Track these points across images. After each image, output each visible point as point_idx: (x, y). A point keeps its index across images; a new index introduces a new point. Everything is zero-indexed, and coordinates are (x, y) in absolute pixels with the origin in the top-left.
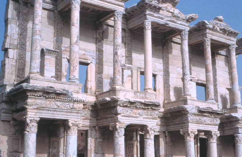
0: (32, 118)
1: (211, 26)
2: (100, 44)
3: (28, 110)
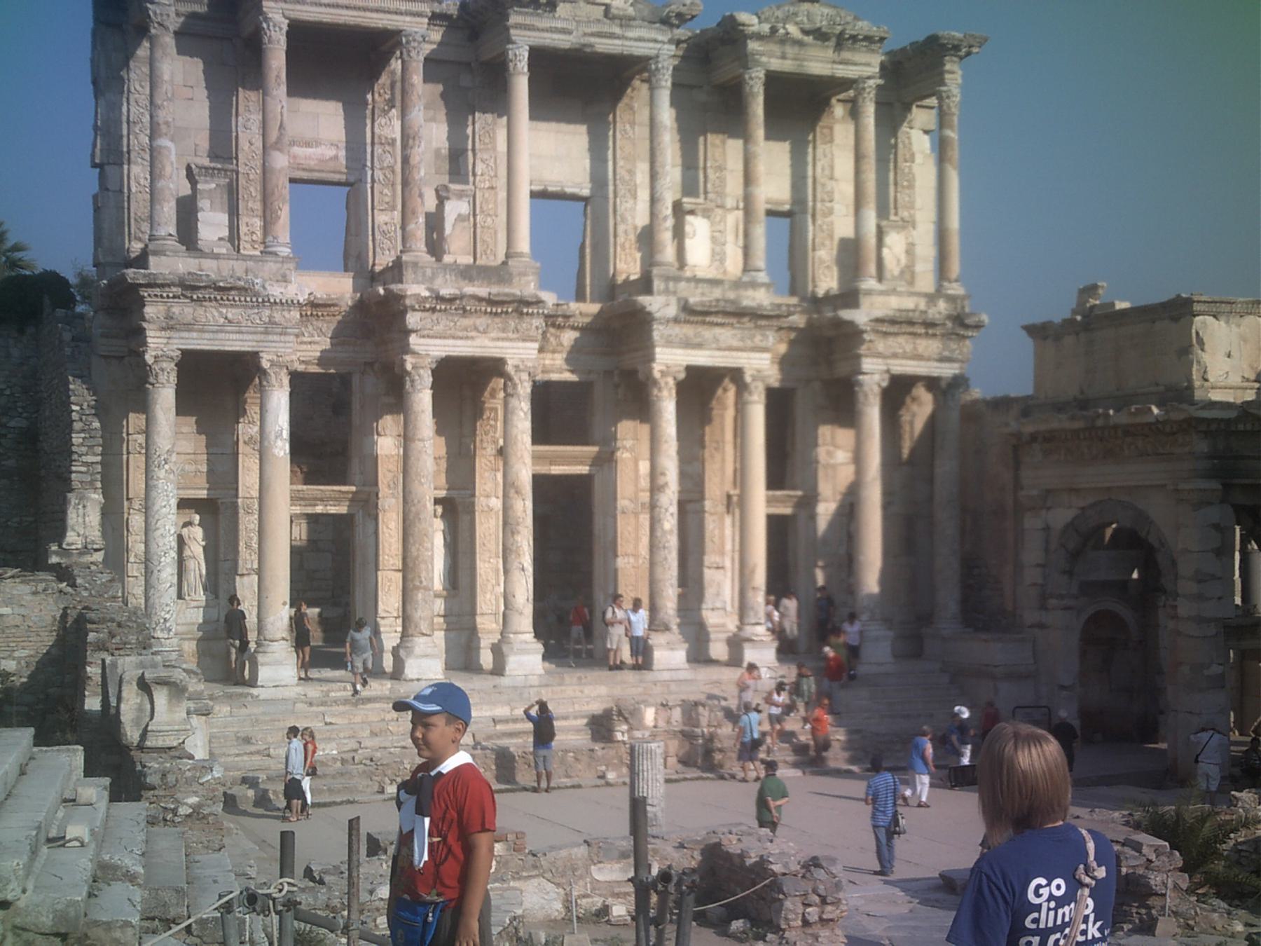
0: (160, 353)
1: (766, 28)
2: (383, 121)
3: (149, 333)
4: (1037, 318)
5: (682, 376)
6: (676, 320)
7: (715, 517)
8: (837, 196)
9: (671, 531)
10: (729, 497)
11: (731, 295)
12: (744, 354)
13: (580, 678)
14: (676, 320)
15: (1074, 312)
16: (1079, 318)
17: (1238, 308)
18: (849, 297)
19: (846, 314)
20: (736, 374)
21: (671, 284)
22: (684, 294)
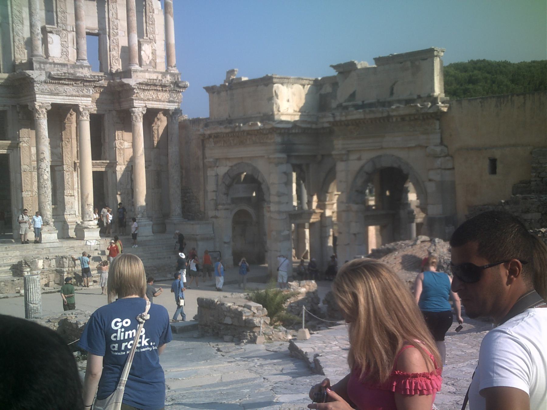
4: (210, 84)
5: (50, 108)
6: (45, 82)
7: (69, 173)
8: (119, 27)
9: (48, 179)
10: (75, 163)
11: (72, 71)
12: (79, 98)
13: (6, 248)
14: (45, 82)
15: (225, 81)
16: (227, 84)
17: (291, 81)
18: (127, 73)
19: (125, 81)
20: (75, 108)
21: (42, 65)
22: (49, 70)
